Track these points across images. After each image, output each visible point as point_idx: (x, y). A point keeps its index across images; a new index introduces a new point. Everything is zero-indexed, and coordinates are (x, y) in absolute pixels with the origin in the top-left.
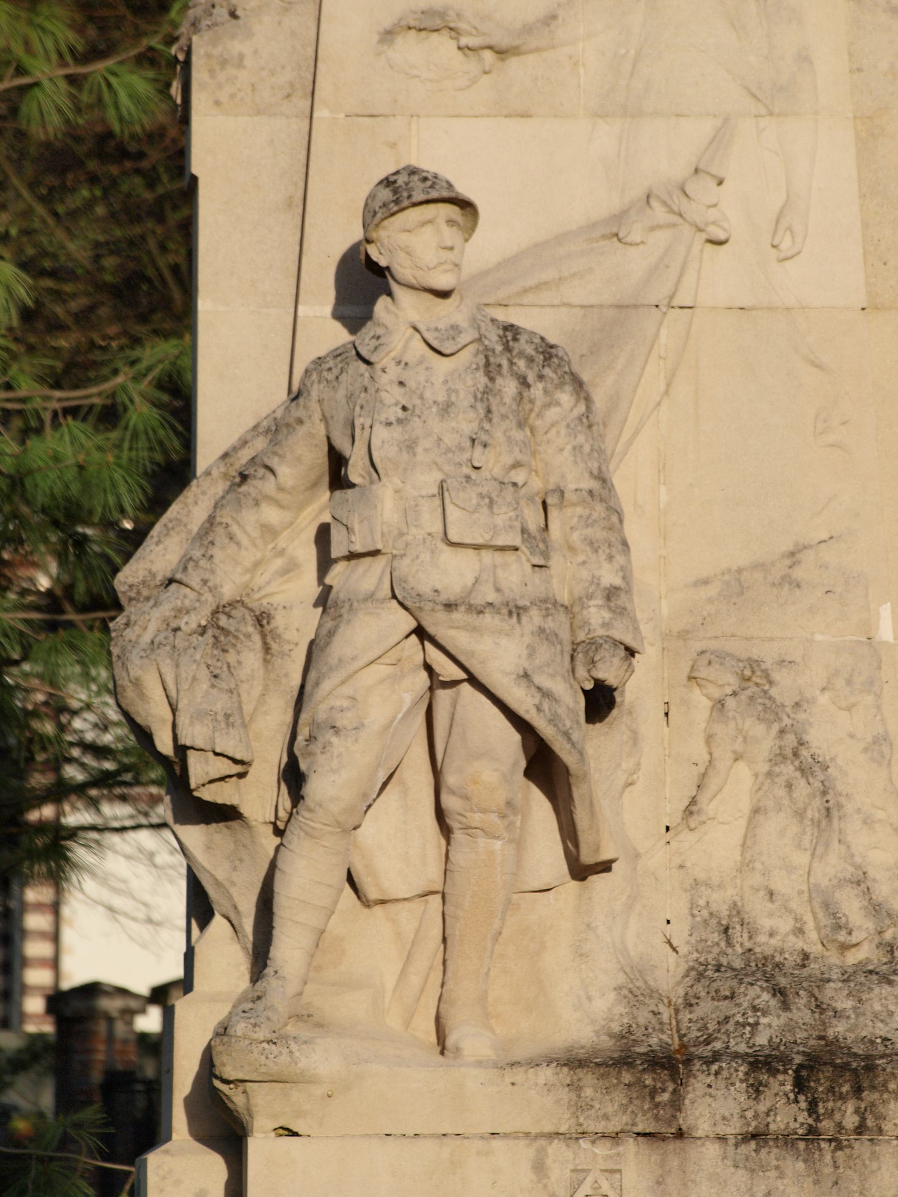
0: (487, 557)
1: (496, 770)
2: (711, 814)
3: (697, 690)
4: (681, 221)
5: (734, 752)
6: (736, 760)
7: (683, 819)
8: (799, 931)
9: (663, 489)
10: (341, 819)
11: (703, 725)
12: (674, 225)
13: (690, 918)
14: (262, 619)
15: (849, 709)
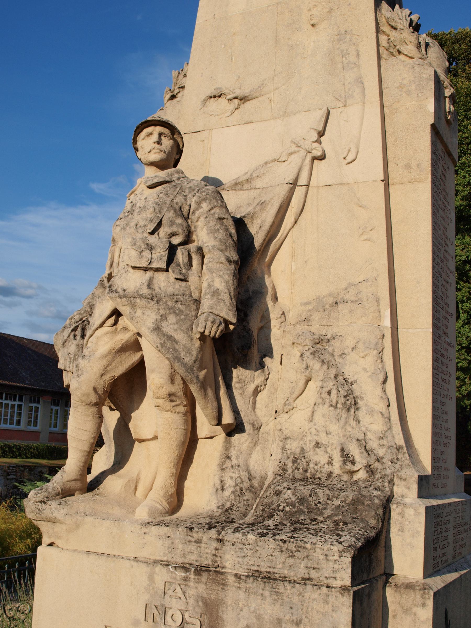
0: (149, 274)
1: (162, 378)
2: (295, 405)
4: (301, 149)
8: (330, 463)
9: (293, 263)
10: (83, 398)
12: (298, 151)
13: (281, 454)
15: (364, 357)
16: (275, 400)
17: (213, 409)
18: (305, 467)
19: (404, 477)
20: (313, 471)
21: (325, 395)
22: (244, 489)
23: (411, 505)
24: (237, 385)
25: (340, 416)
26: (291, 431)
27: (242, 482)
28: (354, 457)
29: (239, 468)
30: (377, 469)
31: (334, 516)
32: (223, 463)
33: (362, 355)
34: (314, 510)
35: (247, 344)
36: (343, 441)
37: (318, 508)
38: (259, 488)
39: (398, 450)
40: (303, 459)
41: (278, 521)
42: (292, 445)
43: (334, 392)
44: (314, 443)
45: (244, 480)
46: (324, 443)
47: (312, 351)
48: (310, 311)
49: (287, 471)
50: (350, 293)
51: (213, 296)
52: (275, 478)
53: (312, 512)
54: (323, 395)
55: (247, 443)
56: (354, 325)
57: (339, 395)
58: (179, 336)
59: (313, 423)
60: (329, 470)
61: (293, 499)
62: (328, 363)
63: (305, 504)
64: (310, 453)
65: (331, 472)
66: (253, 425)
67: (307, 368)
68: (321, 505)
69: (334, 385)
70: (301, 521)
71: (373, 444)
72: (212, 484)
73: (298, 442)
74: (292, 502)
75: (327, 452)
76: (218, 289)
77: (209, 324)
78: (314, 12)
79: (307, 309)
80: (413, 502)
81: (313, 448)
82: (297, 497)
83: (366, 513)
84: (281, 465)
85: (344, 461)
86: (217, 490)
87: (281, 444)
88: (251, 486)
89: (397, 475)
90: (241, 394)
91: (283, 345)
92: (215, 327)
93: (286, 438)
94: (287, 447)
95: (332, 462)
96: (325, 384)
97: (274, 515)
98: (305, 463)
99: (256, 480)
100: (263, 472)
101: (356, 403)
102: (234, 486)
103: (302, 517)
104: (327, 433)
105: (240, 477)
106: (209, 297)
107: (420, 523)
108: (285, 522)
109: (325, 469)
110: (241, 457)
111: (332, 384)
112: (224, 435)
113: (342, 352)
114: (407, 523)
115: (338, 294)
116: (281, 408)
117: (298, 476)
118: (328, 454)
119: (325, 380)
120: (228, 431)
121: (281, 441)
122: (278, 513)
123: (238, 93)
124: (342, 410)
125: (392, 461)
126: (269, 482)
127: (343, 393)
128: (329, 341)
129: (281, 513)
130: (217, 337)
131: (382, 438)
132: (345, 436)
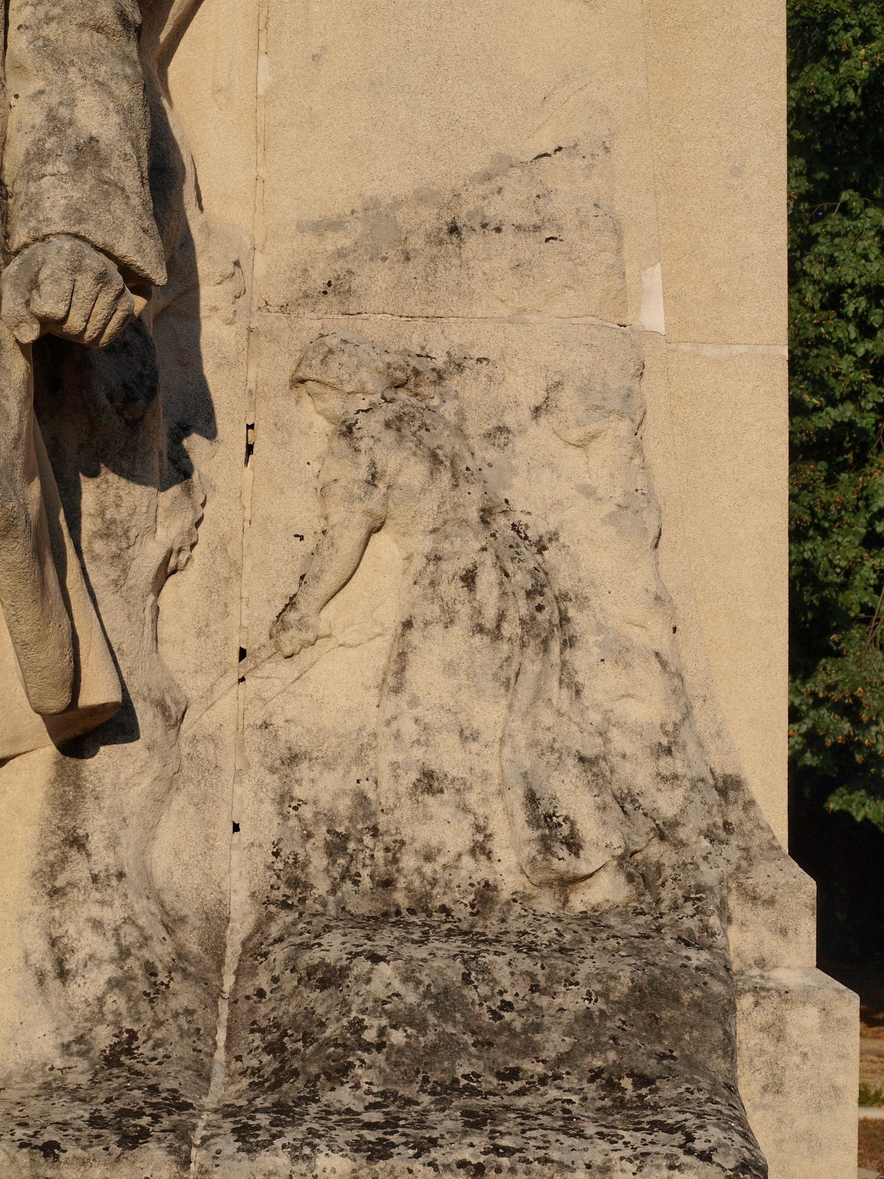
2: (323, 629)
3: (307, 401)
5: (368, 513)
6: (376, 530)
7: (271, 637)
9: (264, 60)
11: (316, 466)
13: (278, 820)
15: (581, 445)
16: (233, 609)
17: (62, 647)
18: (382, 869)
19: (765, 891)
20: (417, 883)
21: (453, 590)
22: (160, 966)
23: (807, 996)
24: (99, 546)
25: (515, 667)
26: (309, 731)
27: (145, 940)
28: (573, 824)
29: (123, 886)
30: (659, 867)
31: (583, 1056)
32: (53, 869)
33: (575, 435)
34: (498, 1034)
35: (140, 375)
36: (528, 764)
37: (508, 1027)
38: (208, 961)
39: (723, 792)
40: (368, 840)
41: (375, 1089)
42: (320, 785)
43: (487, 577)
44: (414, 776)
45: (148, 932)
46: (453, 773)
47: (390, 416)
48: (341, 254)
49: (308, 886)
50: (508, 194)
51: (78, 165)
52: (270, 917)
53: (490, 1044)
54: (443, 588)
55: (146, 782)
56: (534, 318)
57: (509, 589)
59: (405, 697)
60: (478, 877)
61: (412, 998)
62: (452, 463)
63: (458, 1015)
64: (397, 813)
65: (487, 884)
66: (162, 706)
67: (373, 479)
68: (514, 1014)
69: (484, 549)
70: (463, 1082)
72: (15, 954)
73: (340, 771)
74: (411, 1009)
75: (465, 809)
76: (92, 139)
77: (86, 282)
79: (330, 248)
80: (808, 981)
81: (412, 795)
82: (422, 989)
83: (696, 1034)
84: (281, 866)
85: (543, 839)
86: (41, 978)
87: (272, 781)
88: (181, 955)
89: (740, 885)
90: (115, 582)
91: (252, 386)
92: (105, 299)
93: (293, 759)
94: (299, 792)
95: (488, 846)
96: (447, 545)
97: (351, 1065)
98: (379, 854)
99: (189, 928)
100: (211, 897)
101: (564, 619)
102: (112, 960)
103: (463, 1068)
104: (467, 736)
105: (129, 920)
106: (64, 169)
107: (842, 1057)
108: (405, 1091)
109: (463, 873)
110: (123, 841)
111: (477, 546)
112: (49, 750)
113: (494, 423)
114: (797, 1059)
115: (458, 196)
116: (264, 638)
117: (361, 906)
118: (471, 817)
119: (448, 529)
120: (70, 734)
121: (273, 770)
122: (365, 1056)
124: (523, 645)
125: (709, 835)
126: (243, 935)
127: (521, 579)
128: (440, 376)
129: (380, 1058)
130: (104, 340)
131: (669, 751)
132: (534, 744)
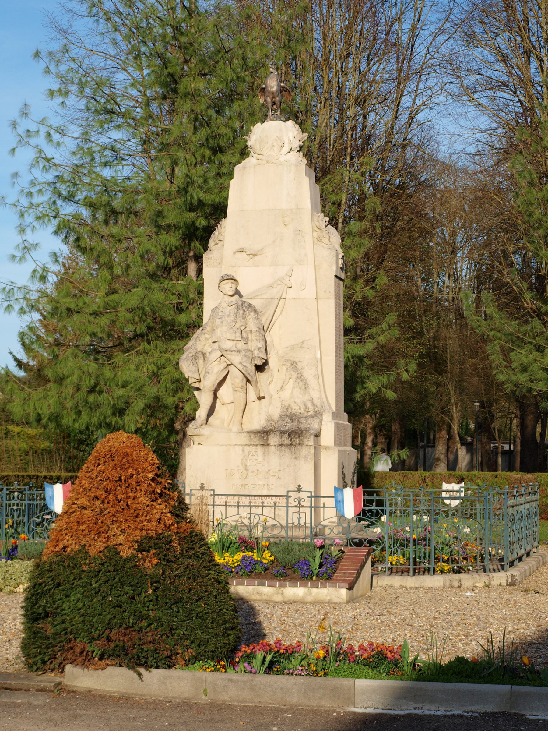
0: (235, 342)
8: (300, 409)
14: (204, 354)
58: (248, 365)
71: (316, 402)
78: (285, 219)
123: (253, 253)
